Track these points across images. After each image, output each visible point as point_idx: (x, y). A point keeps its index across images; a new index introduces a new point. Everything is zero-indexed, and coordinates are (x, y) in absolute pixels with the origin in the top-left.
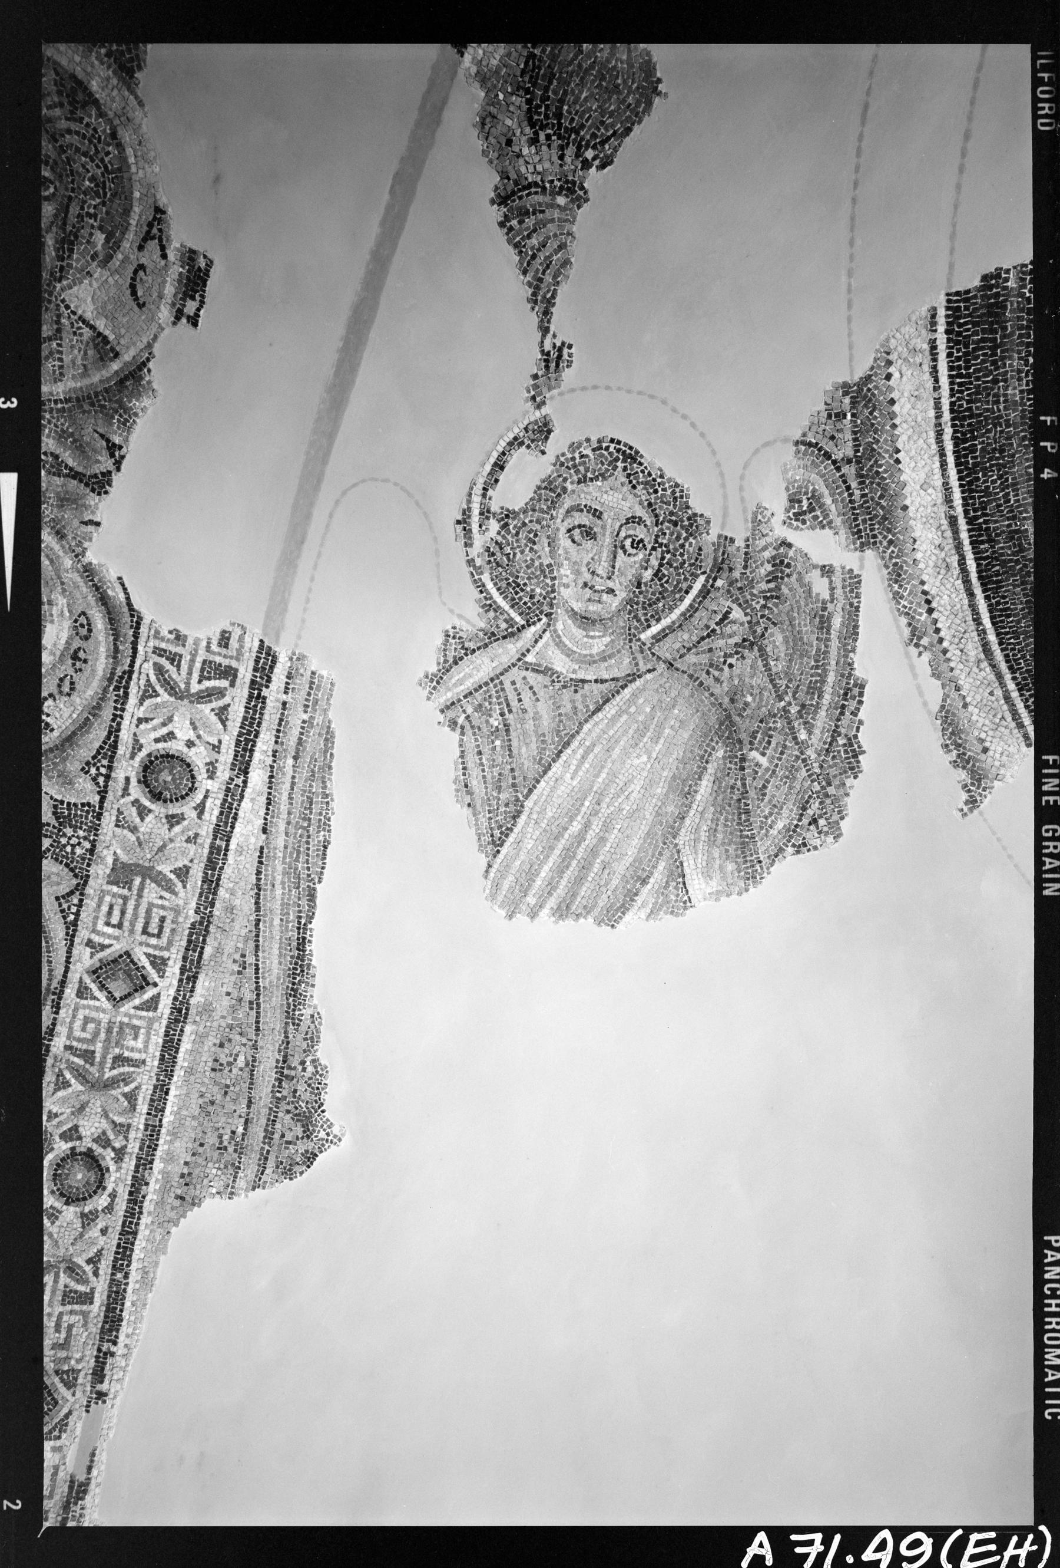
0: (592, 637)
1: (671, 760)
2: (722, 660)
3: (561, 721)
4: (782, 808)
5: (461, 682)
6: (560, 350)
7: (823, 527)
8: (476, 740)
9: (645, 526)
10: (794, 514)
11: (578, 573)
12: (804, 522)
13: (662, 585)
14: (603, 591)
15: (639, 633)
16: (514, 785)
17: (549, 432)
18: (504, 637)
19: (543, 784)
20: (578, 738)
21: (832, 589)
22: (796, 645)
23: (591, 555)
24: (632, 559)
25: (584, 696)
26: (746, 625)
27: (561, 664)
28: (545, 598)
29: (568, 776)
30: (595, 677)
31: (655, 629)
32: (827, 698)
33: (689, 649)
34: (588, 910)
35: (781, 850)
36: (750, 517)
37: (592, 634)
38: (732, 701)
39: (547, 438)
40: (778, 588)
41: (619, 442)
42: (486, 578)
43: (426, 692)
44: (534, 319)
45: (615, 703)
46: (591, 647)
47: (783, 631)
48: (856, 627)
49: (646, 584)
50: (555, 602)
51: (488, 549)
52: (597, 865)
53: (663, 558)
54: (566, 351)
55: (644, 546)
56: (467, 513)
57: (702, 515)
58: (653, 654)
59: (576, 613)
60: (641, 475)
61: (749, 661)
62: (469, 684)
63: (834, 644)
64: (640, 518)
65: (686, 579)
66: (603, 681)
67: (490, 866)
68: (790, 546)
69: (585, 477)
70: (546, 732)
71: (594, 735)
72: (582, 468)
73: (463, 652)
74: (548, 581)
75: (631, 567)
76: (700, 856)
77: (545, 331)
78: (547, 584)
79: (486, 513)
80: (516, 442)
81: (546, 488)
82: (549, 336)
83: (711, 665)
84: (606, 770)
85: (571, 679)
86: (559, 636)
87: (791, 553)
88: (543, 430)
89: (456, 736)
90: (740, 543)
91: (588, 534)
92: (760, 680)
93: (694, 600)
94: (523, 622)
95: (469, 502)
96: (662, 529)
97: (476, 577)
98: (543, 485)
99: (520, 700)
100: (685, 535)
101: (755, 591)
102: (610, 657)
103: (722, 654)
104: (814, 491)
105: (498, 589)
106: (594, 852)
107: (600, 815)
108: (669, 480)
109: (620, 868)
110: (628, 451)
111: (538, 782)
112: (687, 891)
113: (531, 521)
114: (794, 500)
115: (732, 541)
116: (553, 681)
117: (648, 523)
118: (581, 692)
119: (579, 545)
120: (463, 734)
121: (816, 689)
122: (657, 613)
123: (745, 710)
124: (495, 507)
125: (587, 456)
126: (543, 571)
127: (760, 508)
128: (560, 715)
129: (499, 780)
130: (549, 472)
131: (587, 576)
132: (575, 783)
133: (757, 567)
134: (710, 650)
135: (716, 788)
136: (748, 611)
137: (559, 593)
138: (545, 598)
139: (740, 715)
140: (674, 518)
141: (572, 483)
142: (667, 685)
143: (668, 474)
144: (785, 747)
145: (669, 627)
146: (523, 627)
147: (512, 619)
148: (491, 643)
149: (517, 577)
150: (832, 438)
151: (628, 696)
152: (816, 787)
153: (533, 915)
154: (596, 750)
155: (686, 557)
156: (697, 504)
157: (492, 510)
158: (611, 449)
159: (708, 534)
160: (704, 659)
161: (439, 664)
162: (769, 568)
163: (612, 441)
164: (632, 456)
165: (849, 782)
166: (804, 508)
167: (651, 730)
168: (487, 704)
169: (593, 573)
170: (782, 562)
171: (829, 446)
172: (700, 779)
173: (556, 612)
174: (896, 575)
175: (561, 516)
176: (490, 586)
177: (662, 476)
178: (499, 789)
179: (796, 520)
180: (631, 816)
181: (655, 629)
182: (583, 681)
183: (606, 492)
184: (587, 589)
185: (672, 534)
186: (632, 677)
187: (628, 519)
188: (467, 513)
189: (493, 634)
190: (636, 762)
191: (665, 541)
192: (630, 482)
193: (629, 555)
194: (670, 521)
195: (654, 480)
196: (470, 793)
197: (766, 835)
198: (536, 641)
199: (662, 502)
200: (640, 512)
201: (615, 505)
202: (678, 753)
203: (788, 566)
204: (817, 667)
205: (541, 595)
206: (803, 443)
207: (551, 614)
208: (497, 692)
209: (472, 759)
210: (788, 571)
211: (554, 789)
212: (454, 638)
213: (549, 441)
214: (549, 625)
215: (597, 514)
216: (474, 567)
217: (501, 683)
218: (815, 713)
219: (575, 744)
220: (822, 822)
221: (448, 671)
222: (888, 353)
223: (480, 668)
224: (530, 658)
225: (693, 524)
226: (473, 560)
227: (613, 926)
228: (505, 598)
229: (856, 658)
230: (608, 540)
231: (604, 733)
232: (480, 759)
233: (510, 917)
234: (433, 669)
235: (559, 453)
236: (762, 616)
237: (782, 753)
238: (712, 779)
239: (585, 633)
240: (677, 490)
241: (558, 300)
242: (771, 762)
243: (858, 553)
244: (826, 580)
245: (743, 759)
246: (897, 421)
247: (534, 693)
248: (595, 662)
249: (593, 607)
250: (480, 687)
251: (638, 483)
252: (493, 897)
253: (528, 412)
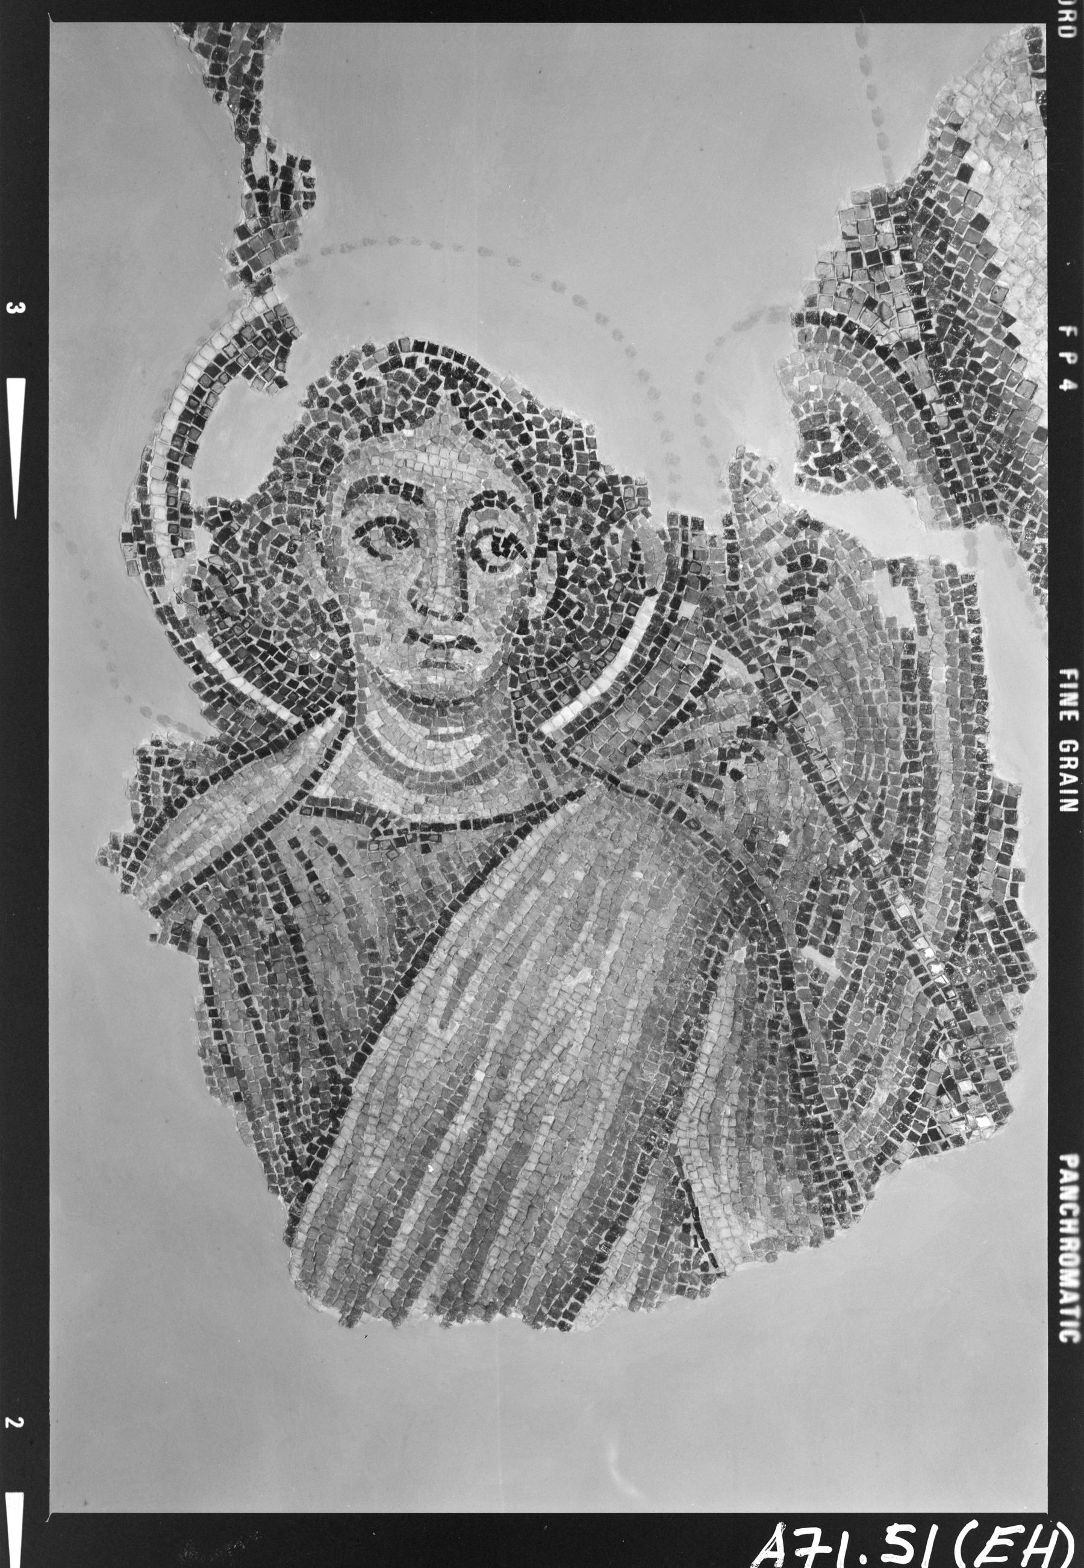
0: (446, 738)
1: (640, 975)
2: (717, 764)
3: (402, 913)
4: (879, 1061)
5: (187, 850)
6: (287, 173)
7: (881, 483)
8: (235, 965)
9: (516, 509)
10: (817, 461)
11: (392, 612)
12: (840, 476)
13: (569, 623)
14: (450, 644)
15: (539, 721)
16: (324, 1050)
17: (288, 339)
18: (263, 753)
19: (383, 1042)
20: (444, 943)
21: (918, 607)
23: (413, 577)
24: (502, 577)
25: (445, 859)
26: (756, 690)
27: (387, 797)
28: (332, 669)
29: (434, 1022)
30: (461, 818)
31: (569, 713)
32: (943, 830)
33: (646, 747)
34: (507, 1297)
35: (889, 1148)
36: (725, 476)
37: (442, 731)
38: (750, 845)
39: (284, 353)
40: (808, 613)
41: (433, 349)
42: (202, 641)
43: (118, 877)
44: (226, 115)
45: (509, 866)
46: (444, 757)
47: (832, 698)
48: (980, 681)
49: (536, 624)
50: (354, 674)
51: (196, 585)
52: (513, 1202)
53: (563, 570)
54: (298, 175)
55: (520, 548)
56: (141, 518)
57: (627, 480)
58: (574, 763)
59: (402, 693)
60: (489, 410)
61: (772, 764)
62: (204, 853)
63: (941, 718)
64: (502, 494)
65: (616, 608)
66: (480, 824)
67: (295, 1220)
68: (817, 526)
69: (375, 422)
70: (376, 936)
71: (476, 934)
72: (365, 407)
73: (182, 788)
74: (333, 635)
75: (501, 592)
76: (724, 1169)
77: (252, 138)
78: (332, 643)
79: (180, 515)
80: (222, 368)
81: (297, 452)
82: (260, 150)
83: (696, 777)
84: (509, 1005)
85: (414, 826)
86: (374, 742)
87: (822, 542)
88: (273, 340)
89: (192, 960)
90: (714, 528)
91: (401, 535)
92: (801, 799)
93: (640, 649)
94: (296, 720)
95: (143, 495)
96: (550, 514)
97: (182, 642)
98: (291, 448)
99: (312, 877)
100: (599, 520)
101: (761, 622)
102: (487, 773)
103: (716, 751)
104: (851, 412)
105: (232, 661)
106: (505, 1176)
107: (509, 1098)
108: (549, 415)
110: (455, 365)
111: (373, 1039)
112: (706, 1245)
113: (277, 521)
114: (813, 434)
115: (698, 525)
116: (376, 833)
117: (521, 503)
118: (436, 850)
119: (386, 557)
120: (204, 954)
121: (917, 810)
122: (569, 680)
123: (778, 863)
124: (198, 501)
125: (372, 382)
126: (318, 617)
127: (743, 460)
128: (399, 900)
129: (294, 1043)
130: (299, 420)
131: (414, 619)
132: (449, 1035)
133: (758, 573)
134: (690, 746)
135: (739, 1026)
136: (754, 661)
137: (360, 657)
138: (332, 669)
139: (769, 874)
140: (570, 489)
141: (351, 437)
142: (612, 821)
143: (545, 403)
144: (869, 934)
145: (598, 706)
146: (298, 728)
147: (272, 716)
148: (237, 766)
149: (267, 634)
150: (870, 304)
151: (534, 852)
152: (945, 1013)
153: (396, 1312)
154: (485, 964)
155: (609, 564)
156: (614, 459)
157: (194, 505)
158: (420, 364)
159: (647, 515)
160: (680, 764)
161: (136, 817)
162: (783, 573)
163: (419, 346)
164: (463, 374)
165: (1011, 1000)
166: (837, 451)
167: (592, 917)
168: (245, 890)
169: (424, 610)
170: (806, 561)
171: (865, 321)
172: (705, 1009)
173: (362, 695)
175: (338, 505)
176: (213, 656)
177: (532, 409)
178: (295, 1059)
179: (824, 473)
181: (569, 713)
182: (439, 827)
183: (424, 449)
184: (418, 643)
185: (572, 521)
186: (536, 813)
187: (477, 499)
188: (141, 518)
189: (239, 748)
190: (571, 983)
191: (560, 537)
192: (470, 425)
193: (493, 569)
194: (564, 496)
195: (518, 417)
196: (235, 1072)
197: (854, 1118)
198: (330, 756)
199: (542, 459)
200: (502, 482)
201: (447, 474)
202: (653, 959)
203: (821, 567)
204: (914, 767)
205: (322, 663)
206: (813, 318)
207: (352, 698)
208: (263, 864)
209: (230, 1006)
210: (821, 577)
211: (407, 1051)
212: (160, 762)
213: (290, 360)
214: (350, 721)
215: (414, 495)
216: (175, 623)
217: (269, 845)
218: (923, 860)
219: (439, 955)
220: (965, 1086)
221: (157, 830)
222: (957, 127)
223: (223, 818)
224: (322, 790)
225: (615, 500)
226: (169, 610)
227: (563, 1326)
228: (249, 677)
229: (990, 742)
230: (443, 544)
231: (496, 929)
232: (248, 1003)
233: (350, 1322)
234: (128, 828)
235: (314, 380)
236: (786, 671)
237: (865, 948)
238: (730, 1008)
239: (427, 732)
240: (568, 433)
241: (266, 76)
242: (845, 968)
243: (962, 530)
244: (903, 591)
245: (788, 965)
246: (997, 261)
247: (341, 861)
248: (457, 787)
249: (436, 678)
250: (228, 857)
251: (486, 425)
252: (309, 1281)
253: (238, 303)
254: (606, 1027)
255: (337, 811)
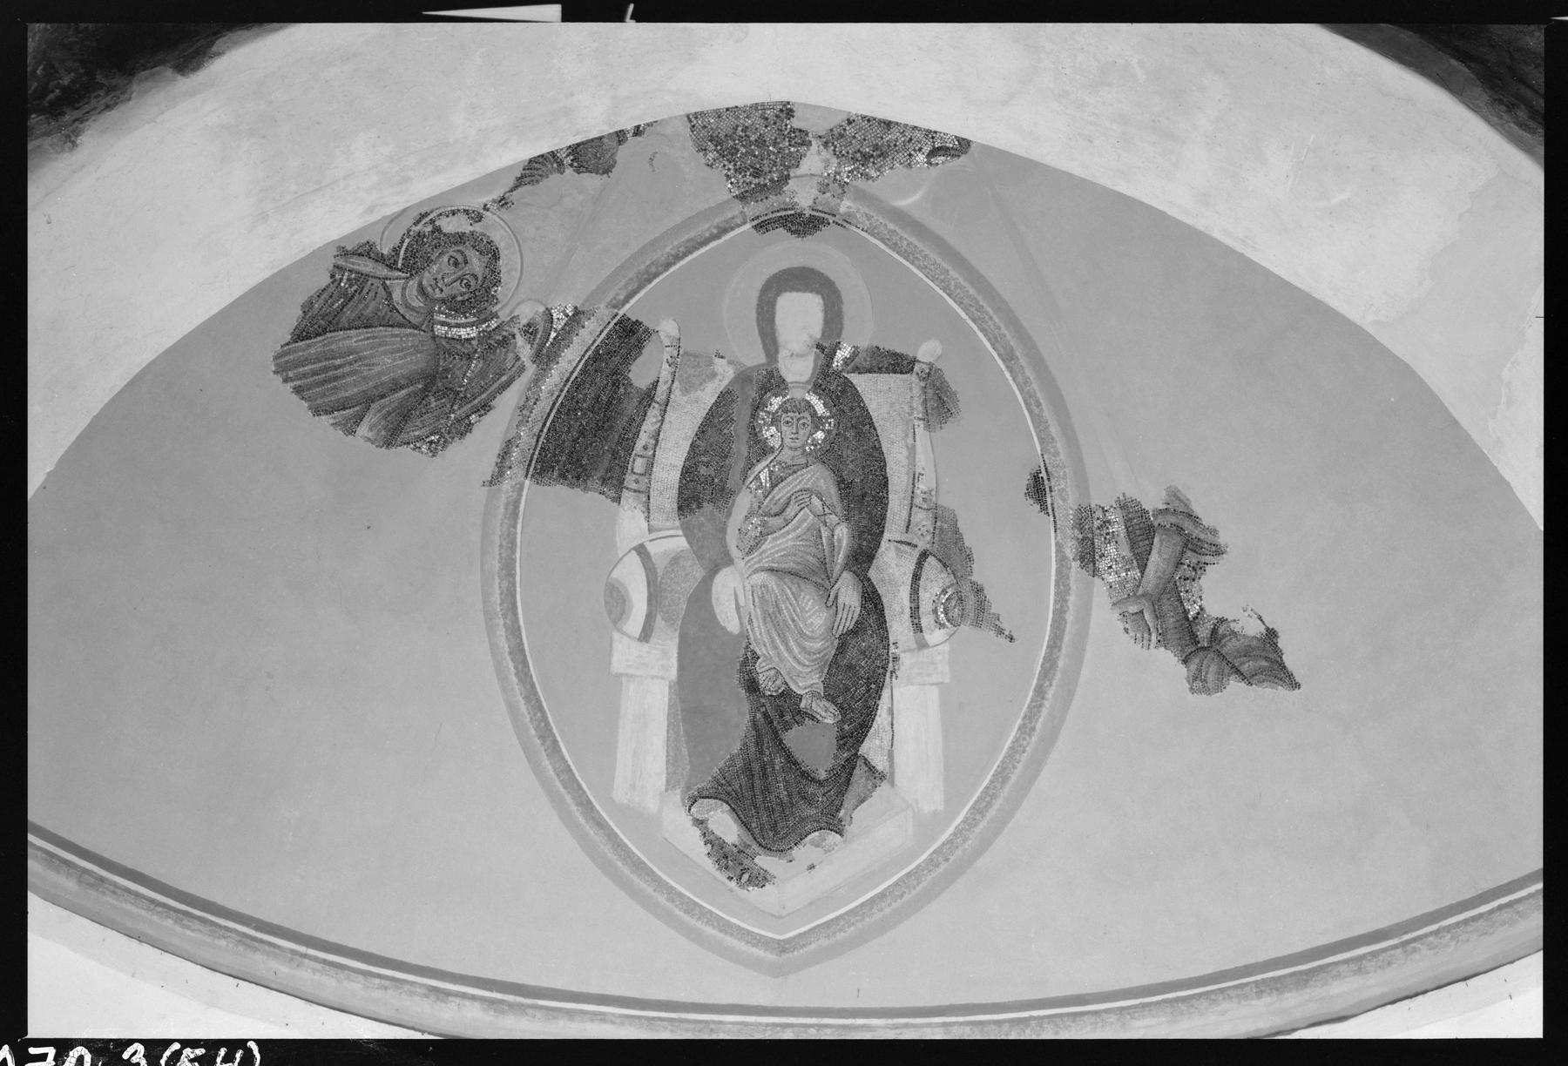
22: (482, 374)
27: (397, 295)
34: (308, 399)
56: (427, 214)
63: (496, 385)
79: (432, 221)
80: (466, 212)
88: (479, 218)
106: (336, 378)
109: (343, 394)
114: (529, 325)
153: (286, 381)
164: (496, 256)
174: (537, 381)
180: (364, 378)
186: (415, 327)
188: (427, 214)
209: (325, 296)
215: (466, 262)
234: (349, 248)
254: (380, 374)
255: (385, 287)
